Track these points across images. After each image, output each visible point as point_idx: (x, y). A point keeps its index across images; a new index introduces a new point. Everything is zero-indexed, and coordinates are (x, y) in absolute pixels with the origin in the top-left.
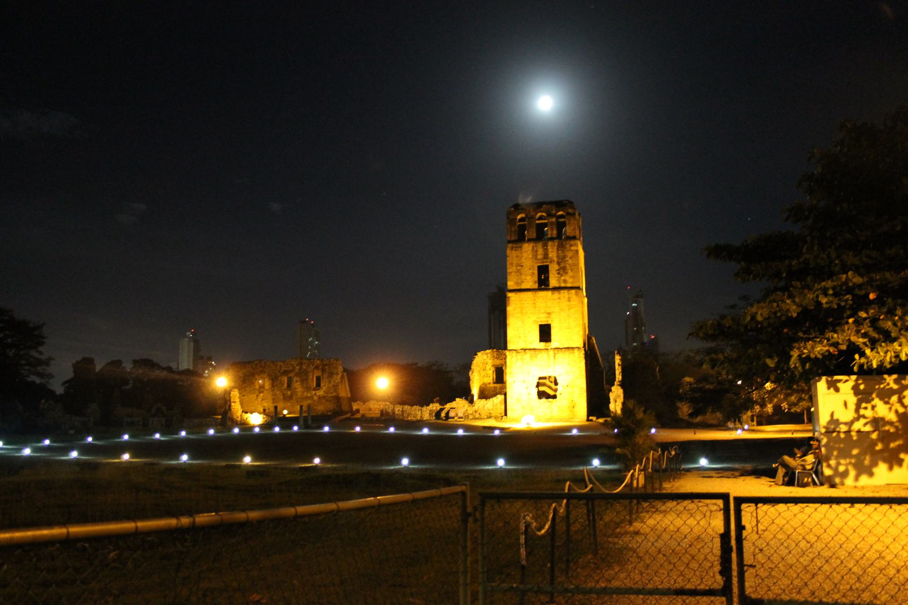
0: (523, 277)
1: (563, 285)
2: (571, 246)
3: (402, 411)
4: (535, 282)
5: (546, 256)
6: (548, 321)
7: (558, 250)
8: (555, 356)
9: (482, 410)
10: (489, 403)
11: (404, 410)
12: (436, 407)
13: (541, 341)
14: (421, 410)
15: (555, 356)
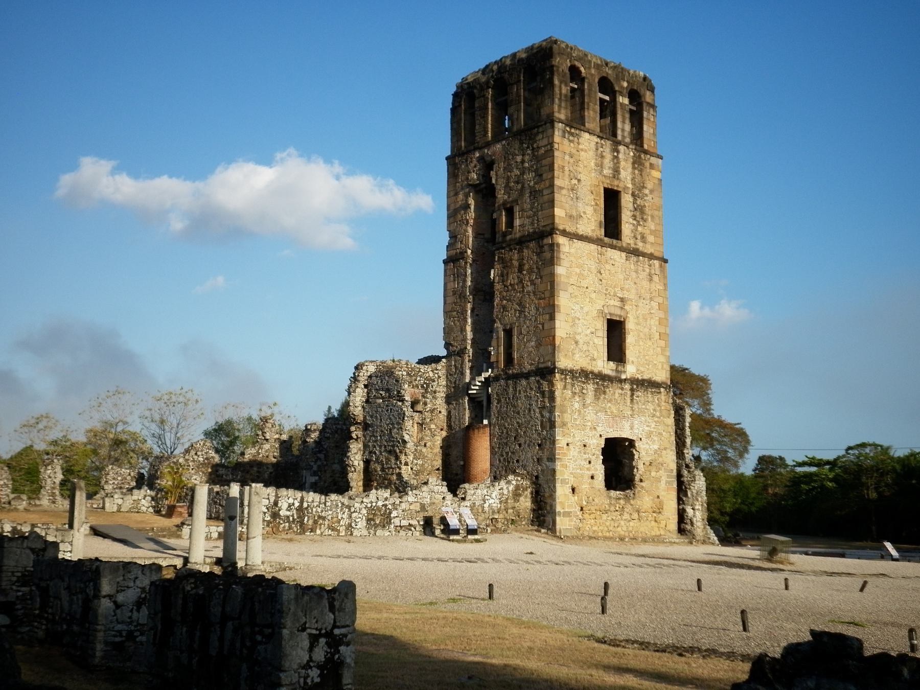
0: (581, 206)
1: (640, 245)
2: (652, 166)
3: (300, 509)
4: (600, 227)
5: (616, 171)
6: (620, 316)
7: (634, 168)
8: (632, 395)
9: (480, 511)
10: (493, 496)
11: (305, 505)
12: (386, 499)
13: (609, 359)
14: (349, 507)
15: (632, 395)
